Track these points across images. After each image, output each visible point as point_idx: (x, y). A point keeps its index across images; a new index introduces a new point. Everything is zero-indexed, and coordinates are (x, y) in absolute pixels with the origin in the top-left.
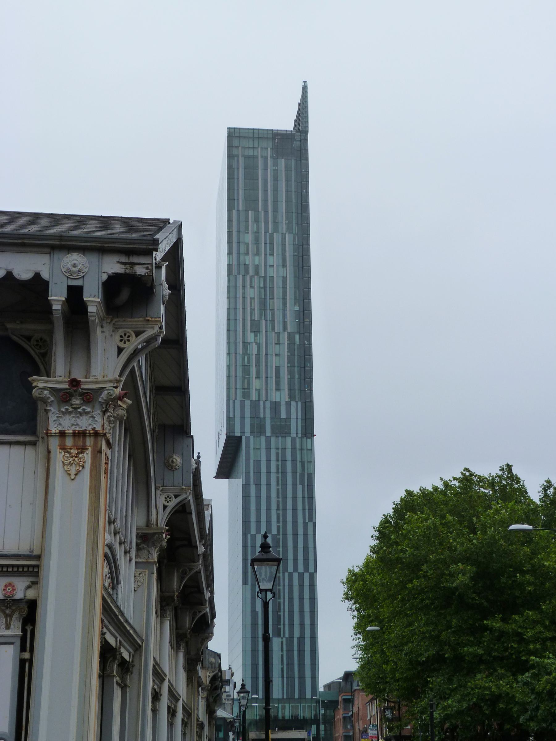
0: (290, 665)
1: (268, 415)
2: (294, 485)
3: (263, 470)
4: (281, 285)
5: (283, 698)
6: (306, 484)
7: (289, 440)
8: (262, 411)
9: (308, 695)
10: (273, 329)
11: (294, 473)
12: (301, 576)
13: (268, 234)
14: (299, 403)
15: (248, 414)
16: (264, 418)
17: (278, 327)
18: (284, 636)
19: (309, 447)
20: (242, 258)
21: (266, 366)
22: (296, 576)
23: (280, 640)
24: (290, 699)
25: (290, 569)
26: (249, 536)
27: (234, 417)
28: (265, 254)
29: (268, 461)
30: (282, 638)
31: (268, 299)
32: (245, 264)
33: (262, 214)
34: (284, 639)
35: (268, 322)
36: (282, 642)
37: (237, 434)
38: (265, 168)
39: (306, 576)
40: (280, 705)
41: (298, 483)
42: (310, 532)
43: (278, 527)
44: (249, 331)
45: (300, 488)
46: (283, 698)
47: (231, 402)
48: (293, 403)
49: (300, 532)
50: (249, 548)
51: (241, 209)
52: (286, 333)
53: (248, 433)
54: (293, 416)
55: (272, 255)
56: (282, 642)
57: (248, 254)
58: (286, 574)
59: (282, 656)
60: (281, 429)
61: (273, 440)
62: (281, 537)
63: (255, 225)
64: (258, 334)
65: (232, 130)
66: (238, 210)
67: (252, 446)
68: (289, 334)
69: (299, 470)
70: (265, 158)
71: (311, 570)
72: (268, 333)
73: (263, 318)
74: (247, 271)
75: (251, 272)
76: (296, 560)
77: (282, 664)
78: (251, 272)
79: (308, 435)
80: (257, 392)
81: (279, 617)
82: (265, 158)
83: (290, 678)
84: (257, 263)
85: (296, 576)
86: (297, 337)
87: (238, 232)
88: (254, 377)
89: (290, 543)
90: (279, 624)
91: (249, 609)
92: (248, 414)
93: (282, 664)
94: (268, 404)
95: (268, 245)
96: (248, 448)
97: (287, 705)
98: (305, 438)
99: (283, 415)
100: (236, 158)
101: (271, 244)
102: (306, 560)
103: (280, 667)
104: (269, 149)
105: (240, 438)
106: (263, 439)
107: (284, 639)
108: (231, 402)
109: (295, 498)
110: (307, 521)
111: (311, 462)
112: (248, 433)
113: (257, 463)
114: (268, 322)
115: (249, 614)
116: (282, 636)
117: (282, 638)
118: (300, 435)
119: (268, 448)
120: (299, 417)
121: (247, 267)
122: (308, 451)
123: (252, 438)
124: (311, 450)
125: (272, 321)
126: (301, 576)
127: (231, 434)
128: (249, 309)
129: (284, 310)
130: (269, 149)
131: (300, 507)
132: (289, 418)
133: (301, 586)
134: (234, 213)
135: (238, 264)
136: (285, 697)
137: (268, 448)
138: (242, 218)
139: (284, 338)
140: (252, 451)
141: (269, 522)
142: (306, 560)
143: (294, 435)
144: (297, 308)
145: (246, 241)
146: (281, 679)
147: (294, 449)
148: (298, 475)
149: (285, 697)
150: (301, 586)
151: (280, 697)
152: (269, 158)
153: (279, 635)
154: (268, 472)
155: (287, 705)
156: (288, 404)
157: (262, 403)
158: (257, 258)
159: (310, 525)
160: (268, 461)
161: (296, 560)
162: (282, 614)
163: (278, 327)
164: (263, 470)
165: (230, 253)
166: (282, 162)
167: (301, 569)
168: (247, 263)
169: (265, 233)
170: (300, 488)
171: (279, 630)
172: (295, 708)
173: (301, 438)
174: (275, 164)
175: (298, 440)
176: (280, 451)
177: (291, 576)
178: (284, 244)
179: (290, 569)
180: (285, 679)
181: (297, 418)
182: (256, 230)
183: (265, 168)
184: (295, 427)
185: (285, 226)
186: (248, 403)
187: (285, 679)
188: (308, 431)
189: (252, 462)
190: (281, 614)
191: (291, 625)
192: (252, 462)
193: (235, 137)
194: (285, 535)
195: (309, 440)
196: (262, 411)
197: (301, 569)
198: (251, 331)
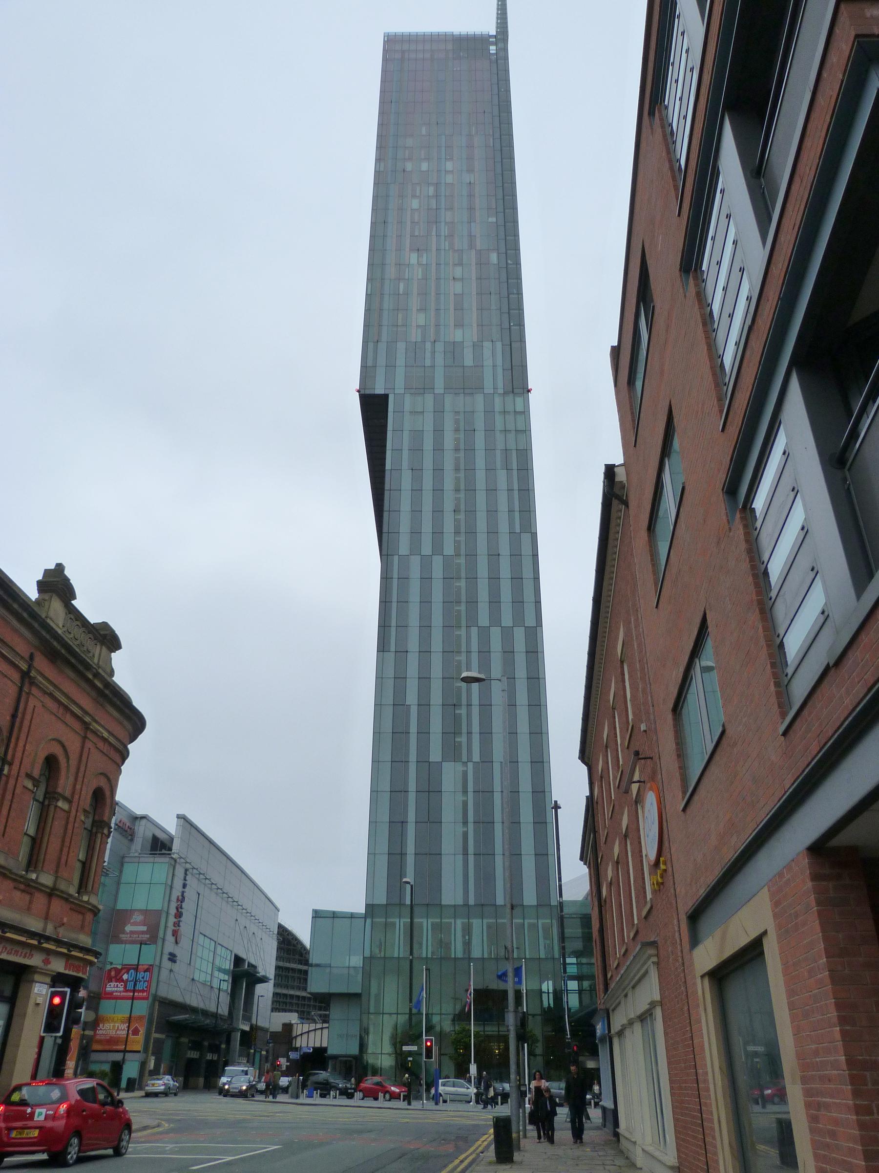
0: (485, 824)
1: (440, 360)
2: (490, 470)
3: (428, 445)
5: (466, 905)
6: (515, 466)
7: (479, 398)
8: (428, 355)
9: (530, 897)
11: (490, 450)
12: (507, 635)
14: (499, 345)
15: (401, 361)
16: (433, 366)
18: (470, 759)
19: (520, 408)
21: (438, 294)
22: (496, 633)
23: (460, 767)
24: (485, 907)
25: (484, 619)
26: (396, 558)
27: (375, 366)
29: (439, 432)
30: (465, 764)
34: (470, 765)
35: (443, 238)
36: (465, 774)
37: (379, 390)
39: (519, 634)
40: (459, 922)
41: (499, 464)
42: (526, 550)
43: (457, 544)
44: (407, 249)
45: (502, 475)
46: (466, 905)
47: (371, 345)
48: (487, 345)
49: (504, 549)
50: (395, 582)
52: (473, 252)
53: (400, 390)
54: (488, 363)
56: (465, 774)
58: (474, 631)
59: (465, 804)
60: (466, 383)
61: (448, 399)
62: (462, 560)
64: (425, 255)
67: (407, 407)
68: (479, 253)
69: (500, 446)
71: (530, 622)
73: (434, 233)
76: (495, 602)
77: (465, 823)
79: (516, 391)
80: (419, 331)
81: (457, 719)
83: (485, 854)
85: (496, 633)
86: (494, 257)
88: (414, 309)
89: (483, 595)
90: (457, 733)
91: (389, 699)
92: (401, 361)
93: (465, 823)
94: (439, 347)
96: (400, 412)
97: (476, 923)
98: (511, 396)
99: (468, 361)
102: (518, 602)
103: (460, 829)
105: (386, 396)
106: (429, 399)
107: (470, 765)
108: (371, 345)
109: (492, 491)
110: (518, 531)
111: (525, 431)
112: (400, 390)
113: (417, 435)
114: (443, 238)
115: (388, 712)
116: (465, 759)
117: (465, 764)
118: (501, 391)
119: (439, 412)
120: (499, 362)
122: (520, 418)
123: (408, 398)
124: (525, 413)
126: (507, 635)
127: (368, 392)
128: (409, 223)
131: (503, 506)
132: (479, 366)
133: (508, 653)
136: (472, 902)
137: (439, 412)
140: (407, 417)
141: (438, 533)
142: (518, 602)
143: (489, 390)
144: (493, 219)
146: (460, 857)
147: (489, 412)
148: (498, 453)
149: (472, 902)
150: (508, 653)
151: (460, 902)
153: (456, 758)
154: (438, 448)
155: (476, 923)
156: (477, 347)
157: (428, 345)
159: (526, 538)
160: (439, 432)
161: (495, 602)
162: (463, 711)
164: (428, 445)
167: (507, 620)
170: (502, 475)
171: (457, 748)
172: (495, 933)
173: (505, 393)
175: (498, 401)
176: (461, 417)
177: (484, 633)
179: (484, 619)
180: (471, 859)
181: (494, 366)
184: (493, 378)
186: (401, 346)
187: (471, 859)
188: (518, 385)
189: (406, 435)
190: (463, 711)
191: (486, 734)
192: (406, 435)
194: (472, 556)
195: (519, 401)
196: (428, 355)
197: (507, 620)
198: (411, 250)
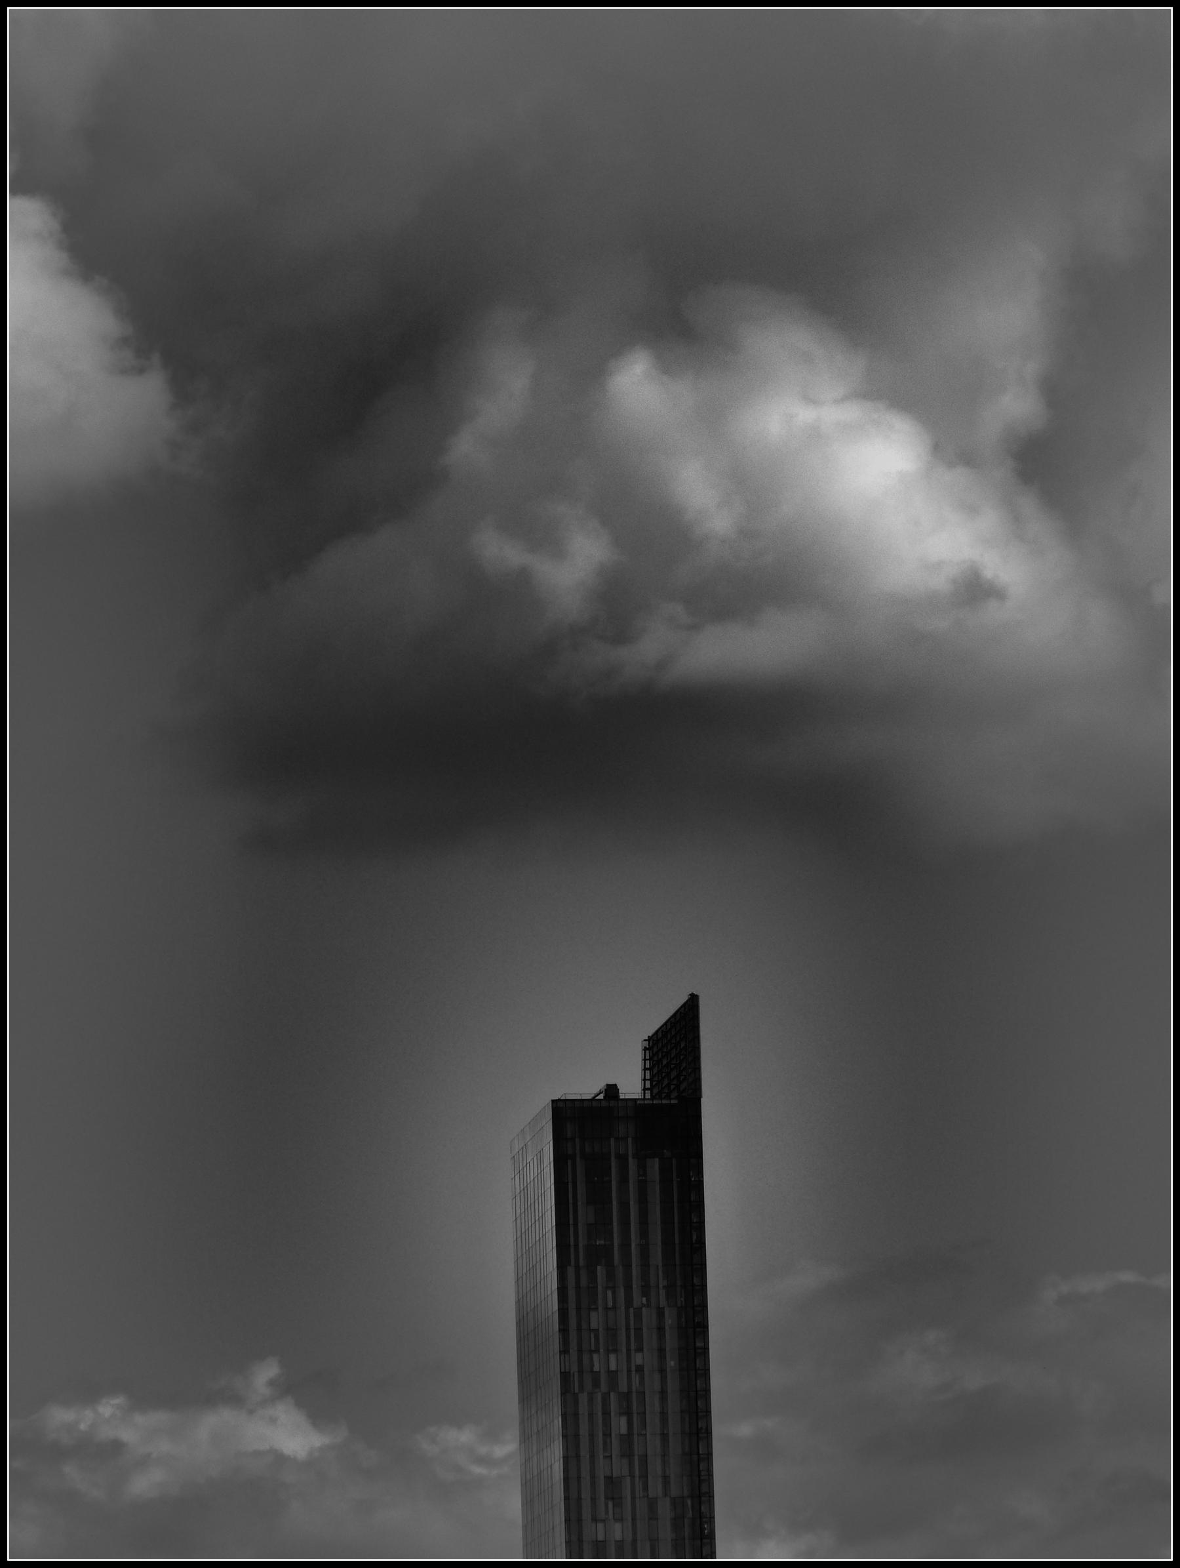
4: (657, 1408)
10: (646, 1488)
13: (631, 1310)
17: (656, 1489)
20: (586, 1358)
28: (628, 1350)
31: (635, 1437)
32: (592, 1371)
33: (620, 1272)
35: (637, 1479)
38: (624, 1180)
51: (582, 1262)
52: (668, 1499)
55: (640, 1349)
57: (597, 1351)
63: (609, 1293)
65: (560, 1105)
66: (577, 1268)
70: (622, 1159)
72: (637, 1501)
74: (596, 1383)
75: (604, 1387)
78: (604, 1387)
82: (622, 1159)
84: (613, 1367)
87: (579, 1309)
95: (632, 1332)
100: (569, 1162)
101: (639, 1330)
104: (630, 1140)
114: (637, 1479)
121: (596, 1377)
125: (644, 1476)
129: (664, 1456)
130: (630, 1140)
134: (571, 1271)
135: (581, 1372)
138: (584, 1282)
139: (665, 1510)
145: (594, 1325)
152: (630, 1159)
158: (612, 1357)
163: (656, 1489)
165: (564, 1351)
166: (654, 1165)
168: (596, 1369)
169: (627, 1309)
174: (642, 1168)
178: (661, 1329)
182: (610, 1304)
183: (624, 1180)
185: (662, 1292)
193: (569, 1118)
198: (607, 1498)
